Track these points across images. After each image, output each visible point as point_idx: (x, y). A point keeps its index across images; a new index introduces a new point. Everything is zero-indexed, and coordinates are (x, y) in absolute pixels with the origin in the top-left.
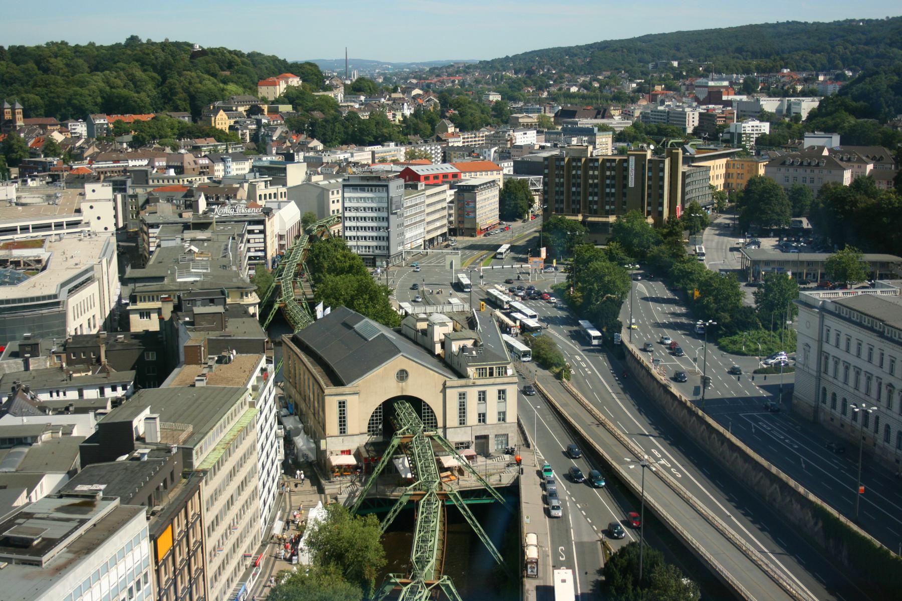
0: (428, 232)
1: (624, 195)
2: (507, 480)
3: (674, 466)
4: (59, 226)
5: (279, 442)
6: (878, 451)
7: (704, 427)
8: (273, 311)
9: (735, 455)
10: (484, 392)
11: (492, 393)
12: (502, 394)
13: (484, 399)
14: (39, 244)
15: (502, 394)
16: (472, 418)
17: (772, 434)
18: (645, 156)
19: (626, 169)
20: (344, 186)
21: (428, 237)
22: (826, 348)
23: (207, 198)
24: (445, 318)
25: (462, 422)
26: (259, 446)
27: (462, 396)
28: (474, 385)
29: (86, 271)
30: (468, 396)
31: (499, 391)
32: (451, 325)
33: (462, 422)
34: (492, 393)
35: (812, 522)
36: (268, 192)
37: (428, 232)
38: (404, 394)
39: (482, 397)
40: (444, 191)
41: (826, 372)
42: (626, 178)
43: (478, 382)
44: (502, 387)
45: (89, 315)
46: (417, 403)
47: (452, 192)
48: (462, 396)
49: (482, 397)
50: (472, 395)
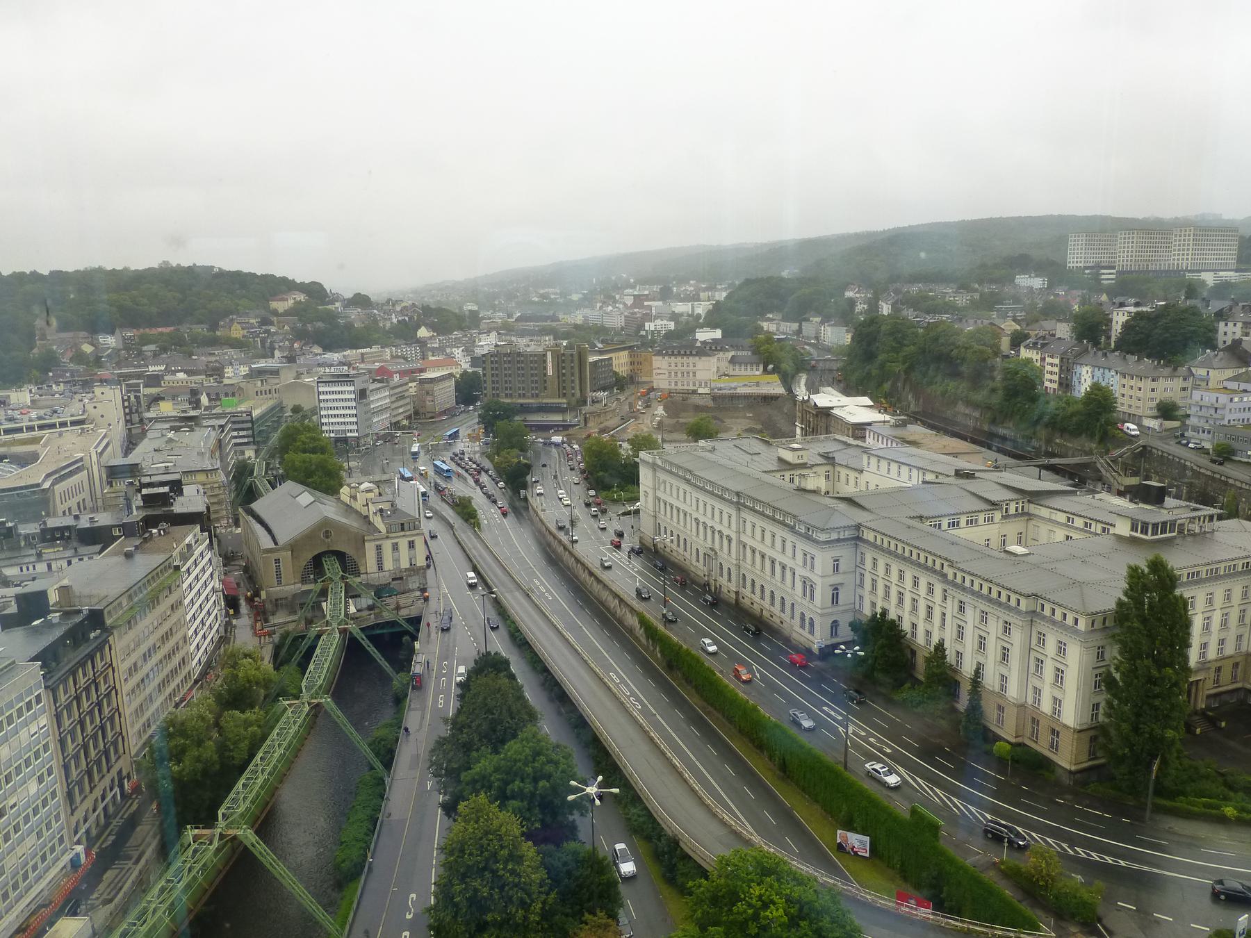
0: (394, 416)
1: (545, 381)
2: (413, 612)
3: (548, 591)
4: (63, 424)
5: (217, 596)
6: (693, 569)
7: (573, 559)
8: (245, 488)
9: (592, 578)
10: (397, 544)
11: (403, 544)
12: (411, 545)
13: (397, 549)
14: (35, 441)
15: (411, 545)
16: (388, 565)
17: (621, 562)
18: (560, 351)
19: (545, 362)
20: (318, 382)
21: (394, 420)
22: (659, 494)
23: (208, 395)
24: (371, 485)
25: (380, 568)
26: (187, 601)
27: (379, 548)
28: (387, 538)
29: (76, 462)
30: (383, 547)
31: (409, 542)
32: (377, 491)
33: (380, 568)
34: (403, 544)
35: (639, 627)
36: (263, 389)
37: (394, 416)
38: (331, 549)
39: (395, 547)
40: (407, 384)
41: (659, 512)
42: (545, 368)
43: (391, 535)
44: (411, 539)
45: (79, 498)
46: (341, 556)
47: (415, 384)
48: (379, 548)
49: (395, 547)
50: (387, 546)
